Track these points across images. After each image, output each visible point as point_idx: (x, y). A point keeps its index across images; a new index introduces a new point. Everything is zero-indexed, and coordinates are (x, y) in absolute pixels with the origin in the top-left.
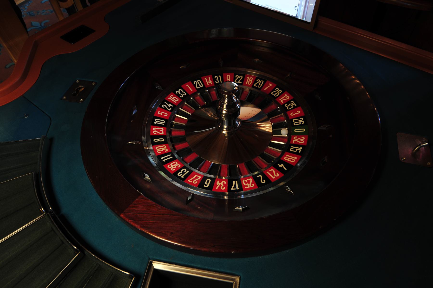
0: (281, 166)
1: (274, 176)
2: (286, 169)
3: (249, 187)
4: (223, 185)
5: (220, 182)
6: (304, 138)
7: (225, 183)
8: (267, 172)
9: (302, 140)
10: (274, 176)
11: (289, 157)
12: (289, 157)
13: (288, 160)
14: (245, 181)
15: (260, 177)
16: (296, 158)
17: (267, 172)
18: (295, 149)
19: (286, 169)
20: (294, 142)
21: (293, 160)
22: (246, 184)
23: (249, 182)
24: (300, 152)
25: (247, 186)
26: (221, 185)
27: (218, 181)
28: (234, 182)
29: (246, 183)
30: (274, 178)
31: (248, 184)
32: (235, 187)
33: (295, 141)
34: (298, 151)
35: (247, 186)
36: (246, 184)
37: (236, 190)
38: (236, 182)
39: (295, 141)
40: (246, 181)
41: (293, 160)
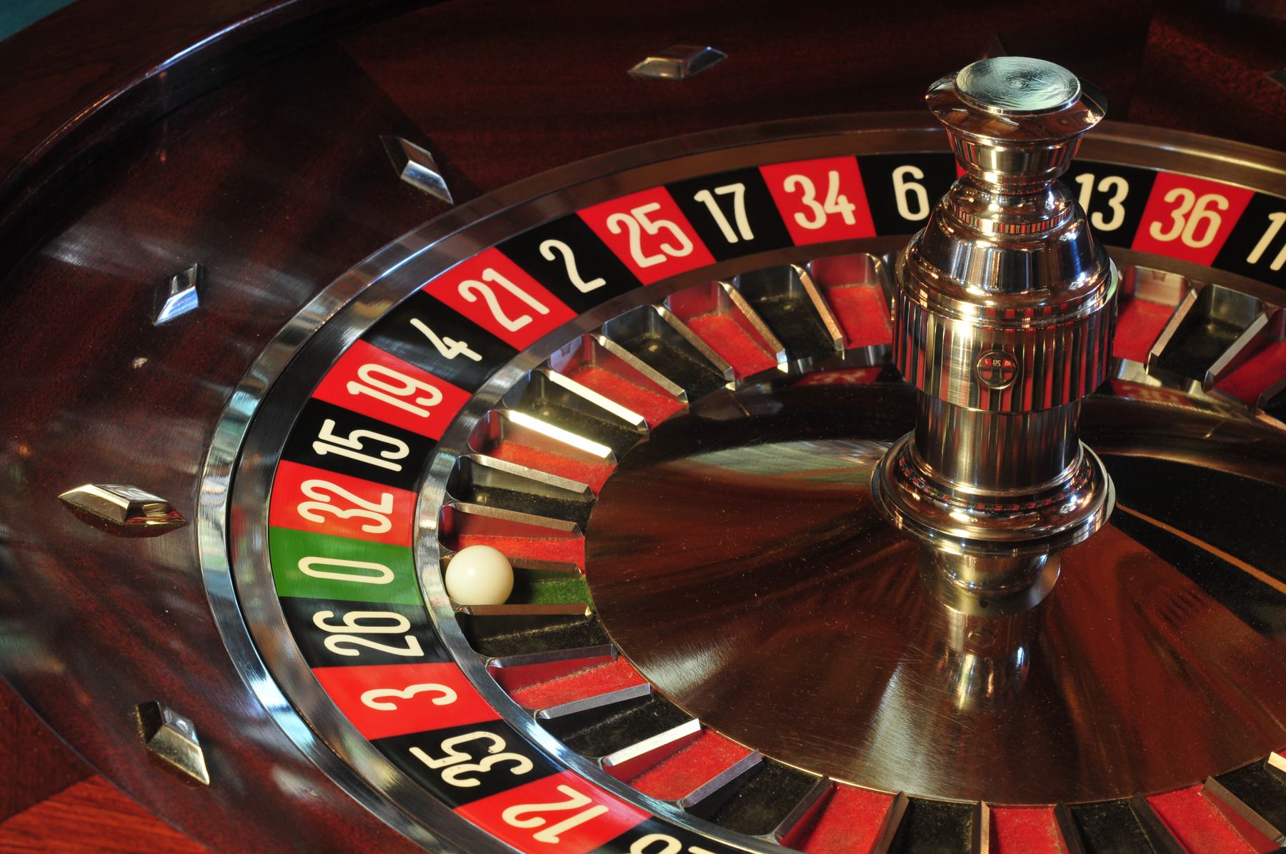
0: (452, 348)
1: (493, 285)
2: (415, 322)
3: (640, 212)
4: (809, 198)
5: (835, 219)
6: (303, 509)
7: (800, 218)
8: (543, 310)
9: (322, 502)
10: (493, 285)
11: (410, 399)
12: (410, 399)
13: (412, 385)
14: (678, 246)
15: (586, 278)
16: (353, 388)
17: (543, 310)
18: (371, 447)
19: (415, 322)
20: (388, 499)
21: (372, 374)
22: (663, 231)
23: (650, 244)
24: (329, 425)
25: (652, 217)
26: (821, 197)
27: (850, 220)
28: (748, 235)
29: (665, 235)
30: (489, 274)
31: (652, 229)
32: (726, 203)
33: (378, 502)
34: (341, 431)
35: (652, 217)
36: (663, 231)
37: (710, 183)
38: (732, 238)
39: (378, 502)
40: (666, 247)
41: (372, 374)
